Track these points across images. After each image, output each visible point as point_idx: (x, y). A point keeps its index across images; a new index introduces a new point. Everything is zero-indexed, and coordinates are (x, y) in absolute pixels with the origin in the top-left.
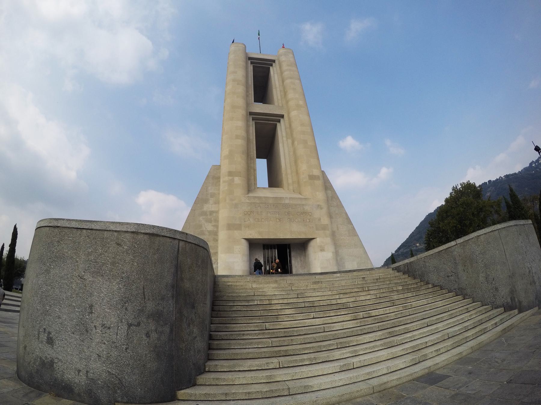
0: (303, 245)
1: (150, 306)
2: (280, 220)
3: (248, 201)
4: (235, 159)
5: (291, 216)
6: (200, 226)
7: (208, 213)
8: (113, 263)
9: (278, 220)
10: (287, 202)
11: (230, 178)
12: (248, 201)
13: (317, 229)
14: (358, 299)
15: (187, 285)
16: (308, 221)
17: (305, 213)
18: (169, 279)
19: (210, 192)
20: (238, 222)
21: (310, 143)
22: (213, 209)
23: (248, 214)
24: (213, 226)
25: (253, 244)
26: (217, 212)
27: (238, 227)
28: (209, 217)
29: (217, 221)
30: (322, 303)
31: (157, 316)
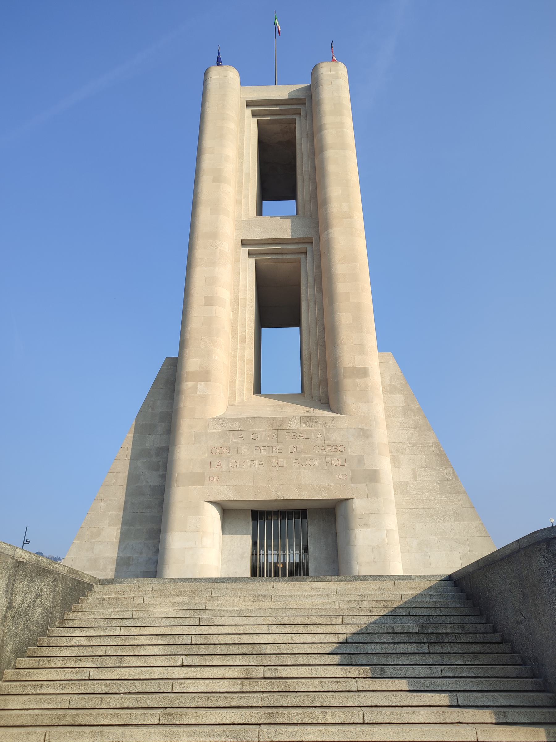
2: (278, 462)
3: (220, 428)
5: (302, 454)
9: (275, 463)
12: (220, 428)
13: (354, 479)
14: (297, 639)
27: (198, 479)
30: (223, 639)
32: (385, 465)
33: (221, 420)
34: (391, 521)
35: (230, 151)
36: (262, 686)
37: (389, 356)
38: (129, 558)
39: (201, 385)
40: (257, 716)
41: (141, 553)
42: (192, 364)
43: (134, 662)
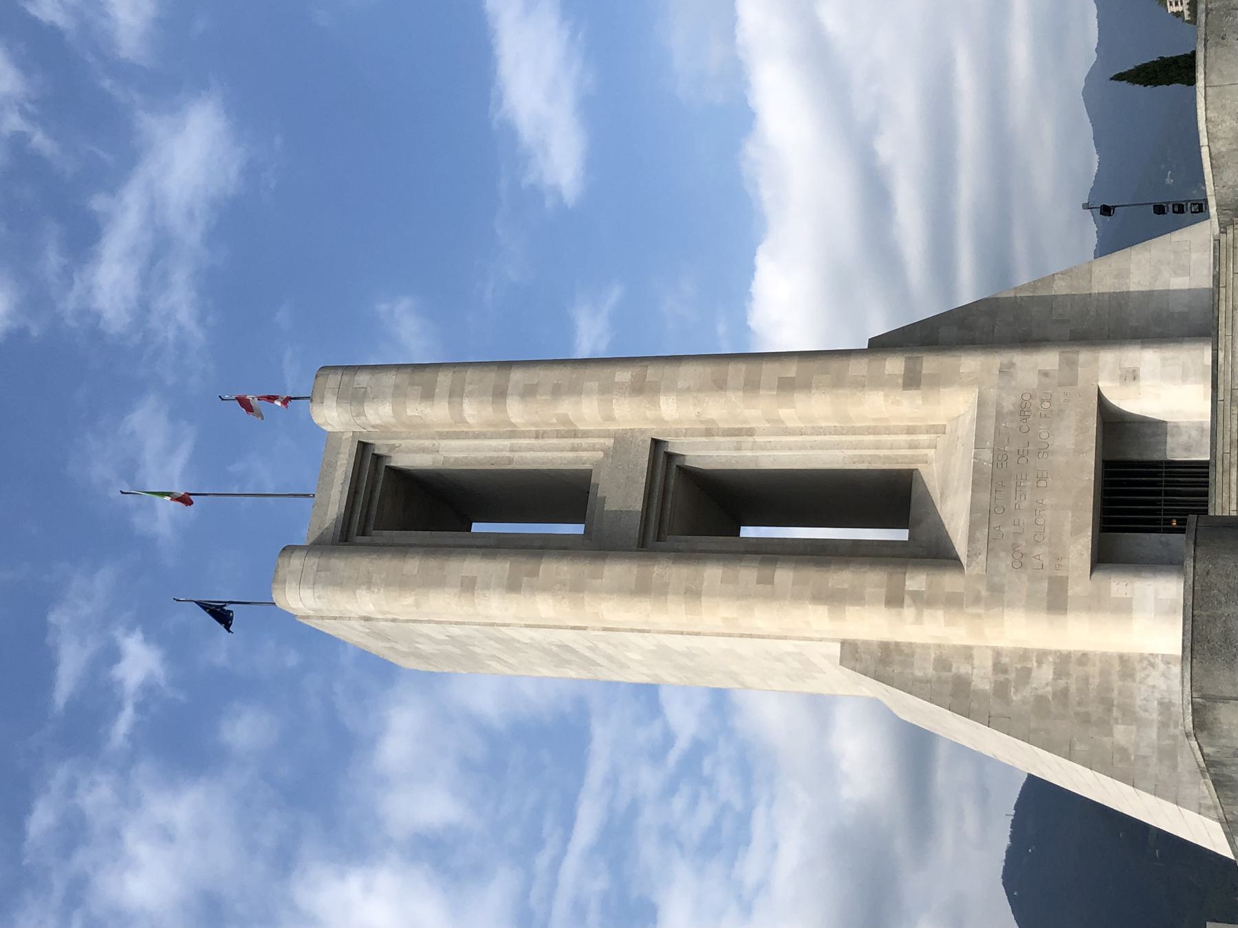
0: (1114, 425)
3: (983, 557)
4: (846, 586)
6: (1040, 700)
7: (1001, 677)
8: (1228, 576)
9: (1043, 483)
10: (987, 455)
11: (908, 600)
13: (1073, 383)
16: (1047, 405)
17: (1023, 411)
19: (930, 672)
20: (1045, 585)
21: (792, 369)
22: (989, 663)
23: (1021, 561)
24: (1040, 663)
25: (1105, 557)
26: (998, 653)
28: (1012, 676)
29: (1025, 655)
38: (1161, 704)
41: (1154, 687)
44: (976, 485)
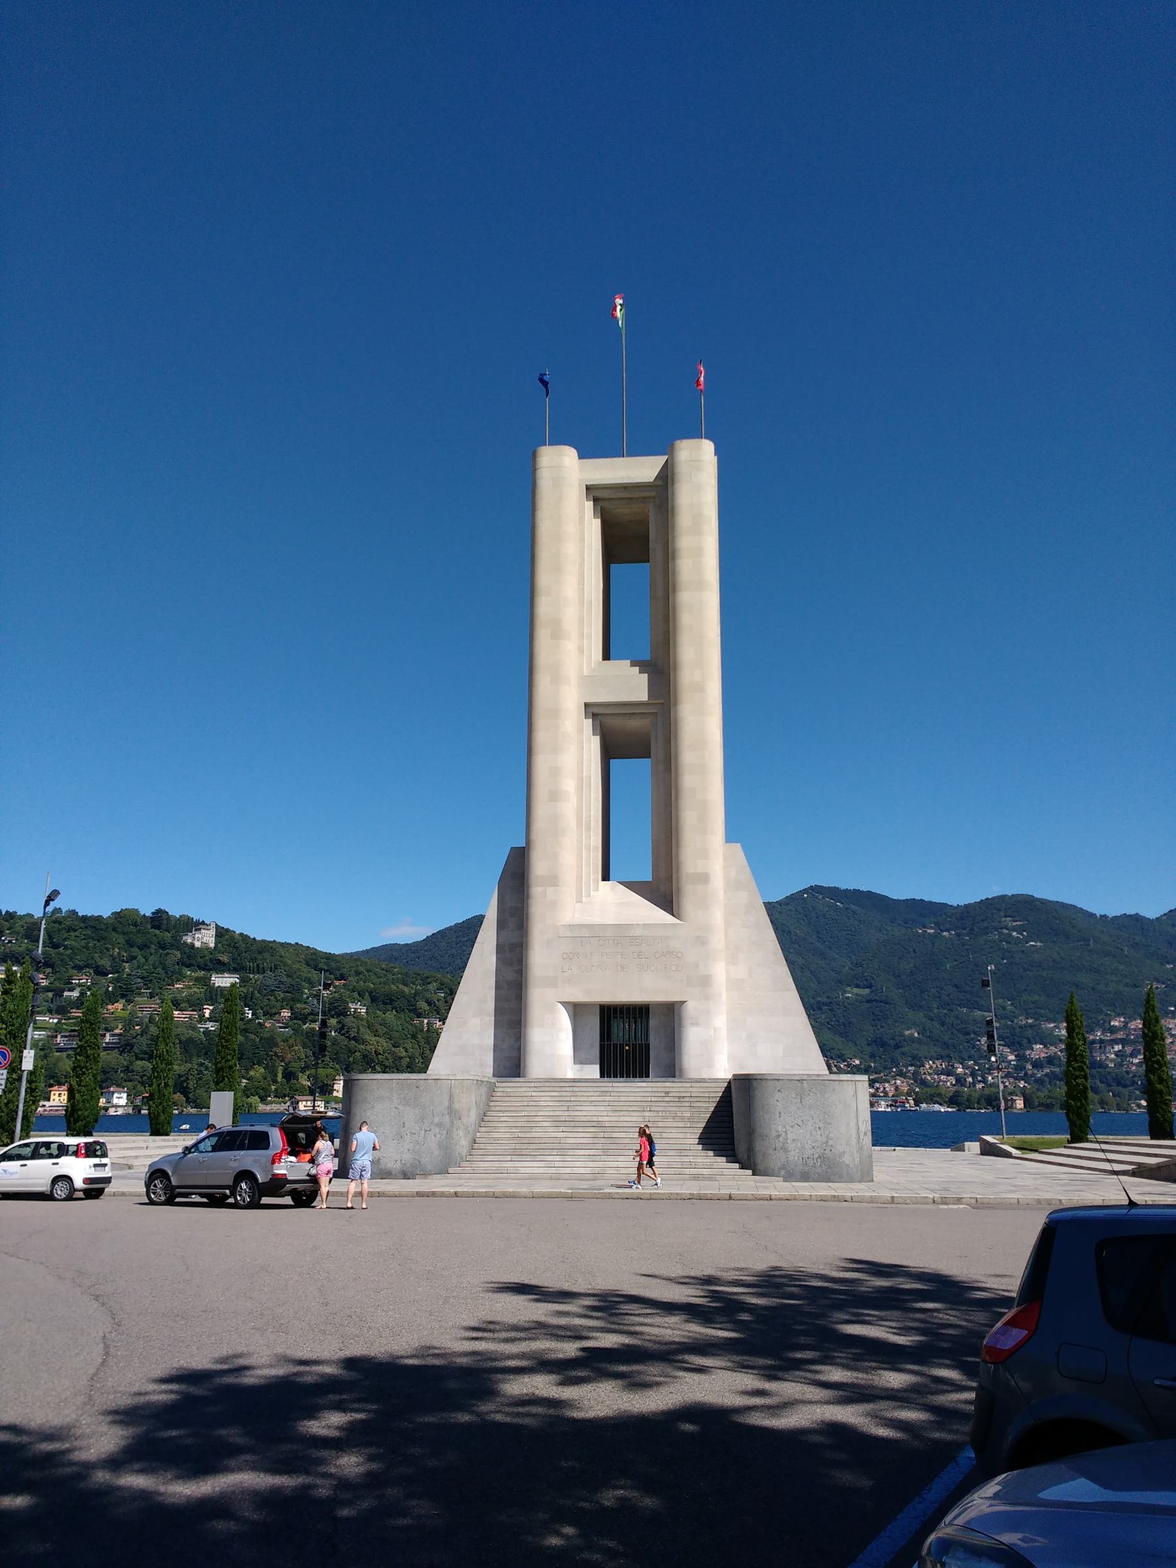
1: (436, 1120)
3: (569, 934)
10: (639, 932)
15: (456, 1106)
18: (446, 1104)
24: (516, 972)
25: (577, 1010)
27: (552, 983)
30: (583, 1119)
31: (440, 1125)
32: (720, 971)
33: (571, 927)
34: (720, 1021)
35: (570, 589)
36: (603, 1141)
37: (737, 848)
39: (550, 890)
40: (600, 1152)
42: (539, 866)
43: (538, 1129)
44: (618, 926)
